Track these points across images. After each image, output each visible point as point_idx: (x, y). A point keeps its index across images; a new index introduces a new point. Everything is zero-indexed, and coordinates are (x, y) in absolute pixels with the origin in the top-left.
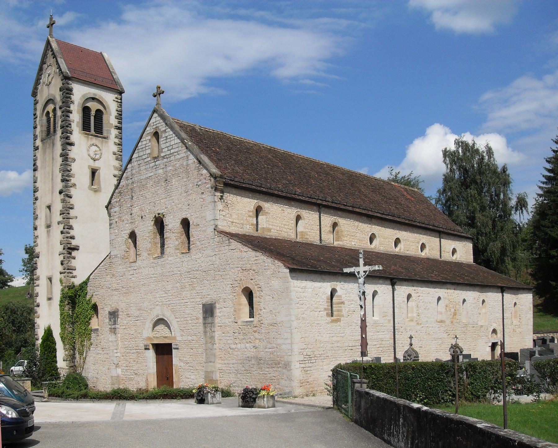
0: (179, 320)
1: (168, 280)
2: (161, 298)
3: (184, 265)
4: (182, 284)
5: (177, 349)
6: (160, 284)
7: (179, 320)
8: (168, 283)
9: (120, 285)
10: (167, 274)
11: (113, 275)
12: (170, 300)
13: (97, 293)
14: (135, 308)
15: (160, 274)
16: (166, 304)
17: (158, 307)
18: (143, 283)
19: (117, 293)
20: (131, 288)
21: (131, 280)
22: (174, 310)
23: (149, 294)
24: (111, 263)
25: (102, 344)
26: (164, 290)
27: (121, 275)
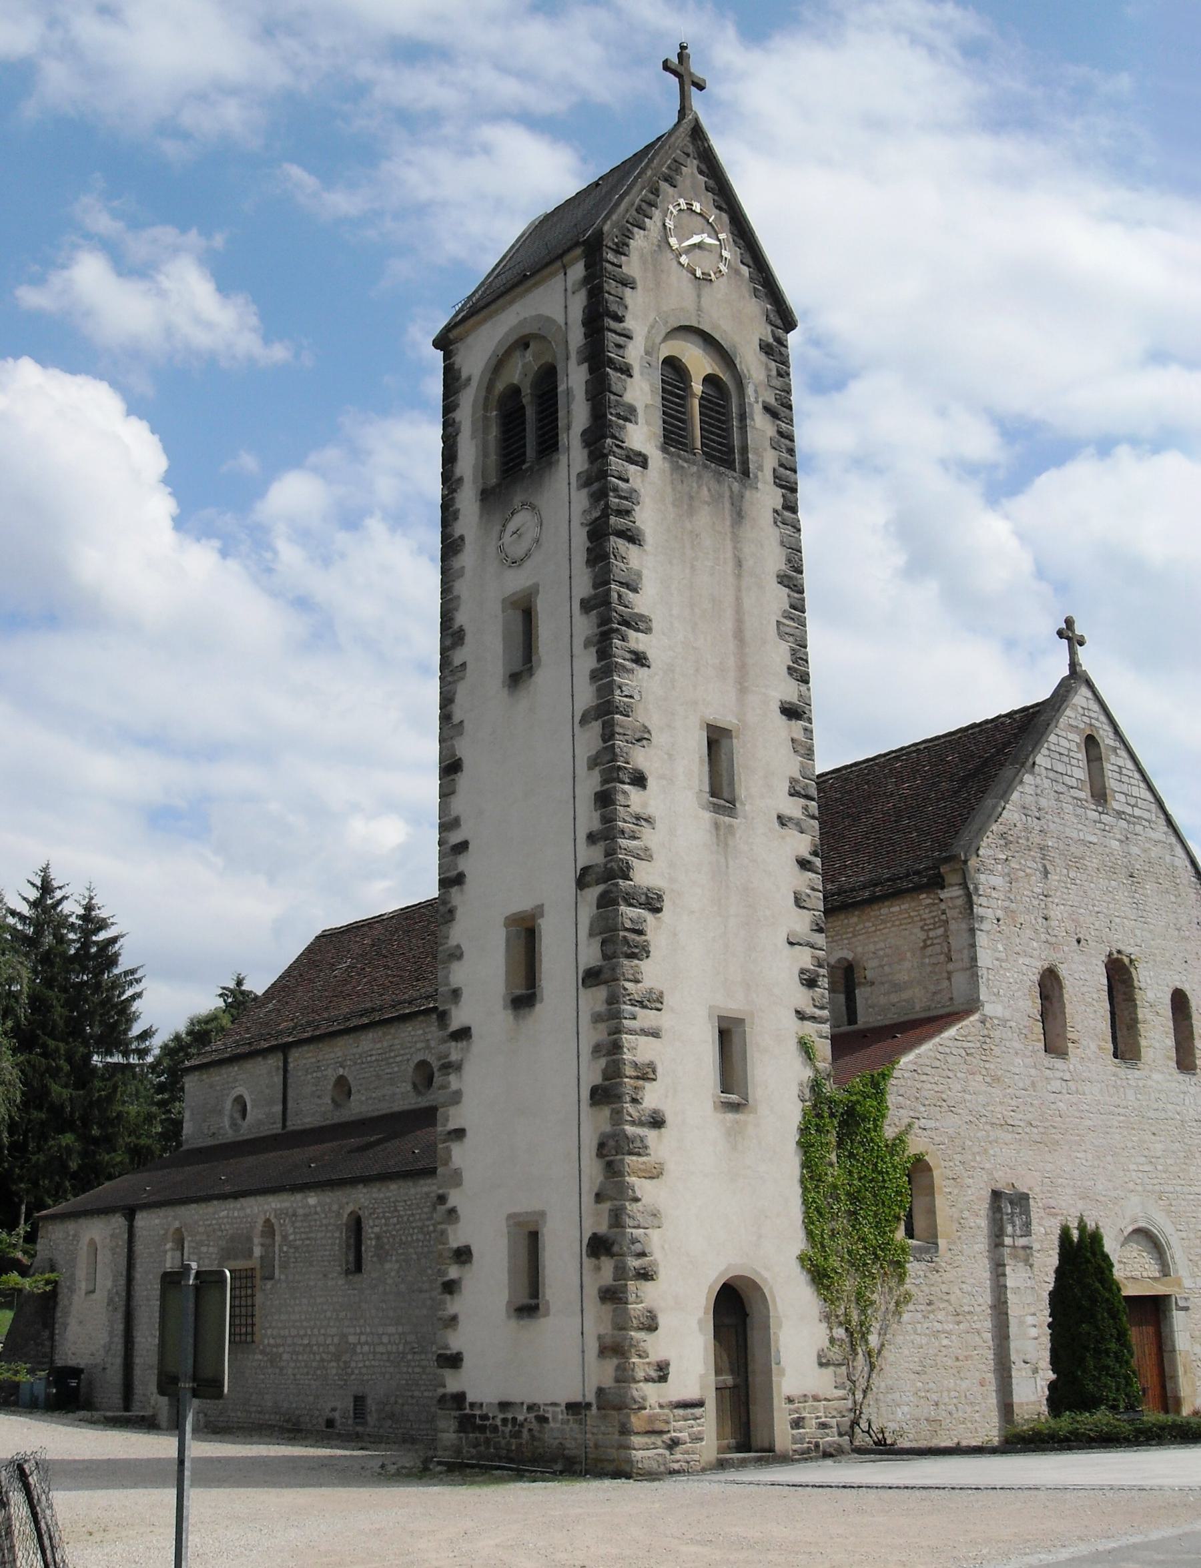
0: (1184, 1235)
1: (1153, 1129)
2: (1140, 1175)
3: (1187, 1102)
4: (1187, 1147)
5: (1186, 1309)
6: (1135, 1136)
7: (1184, 1235)
8: (1153, 1137)
9: (1020, 1116)
10: (1151, 1114)
11: (997, 1079)
12: (1162, 1182)
13: (930, 1124)
14: (1072, 1192)
15: (1134, 1109)
16: (1153, 1192)
17: (1135, 1199)
18: (1091, 1123)
19: (1010, 1136)
20: (1054, 1131)
21: (1053, 1106)
22: (1173, 1209)
23: (1109, 1158)
24: (988, 1040)
25: (952, 1298)
26: (1146, 1153)
27: (1021, 1085)
